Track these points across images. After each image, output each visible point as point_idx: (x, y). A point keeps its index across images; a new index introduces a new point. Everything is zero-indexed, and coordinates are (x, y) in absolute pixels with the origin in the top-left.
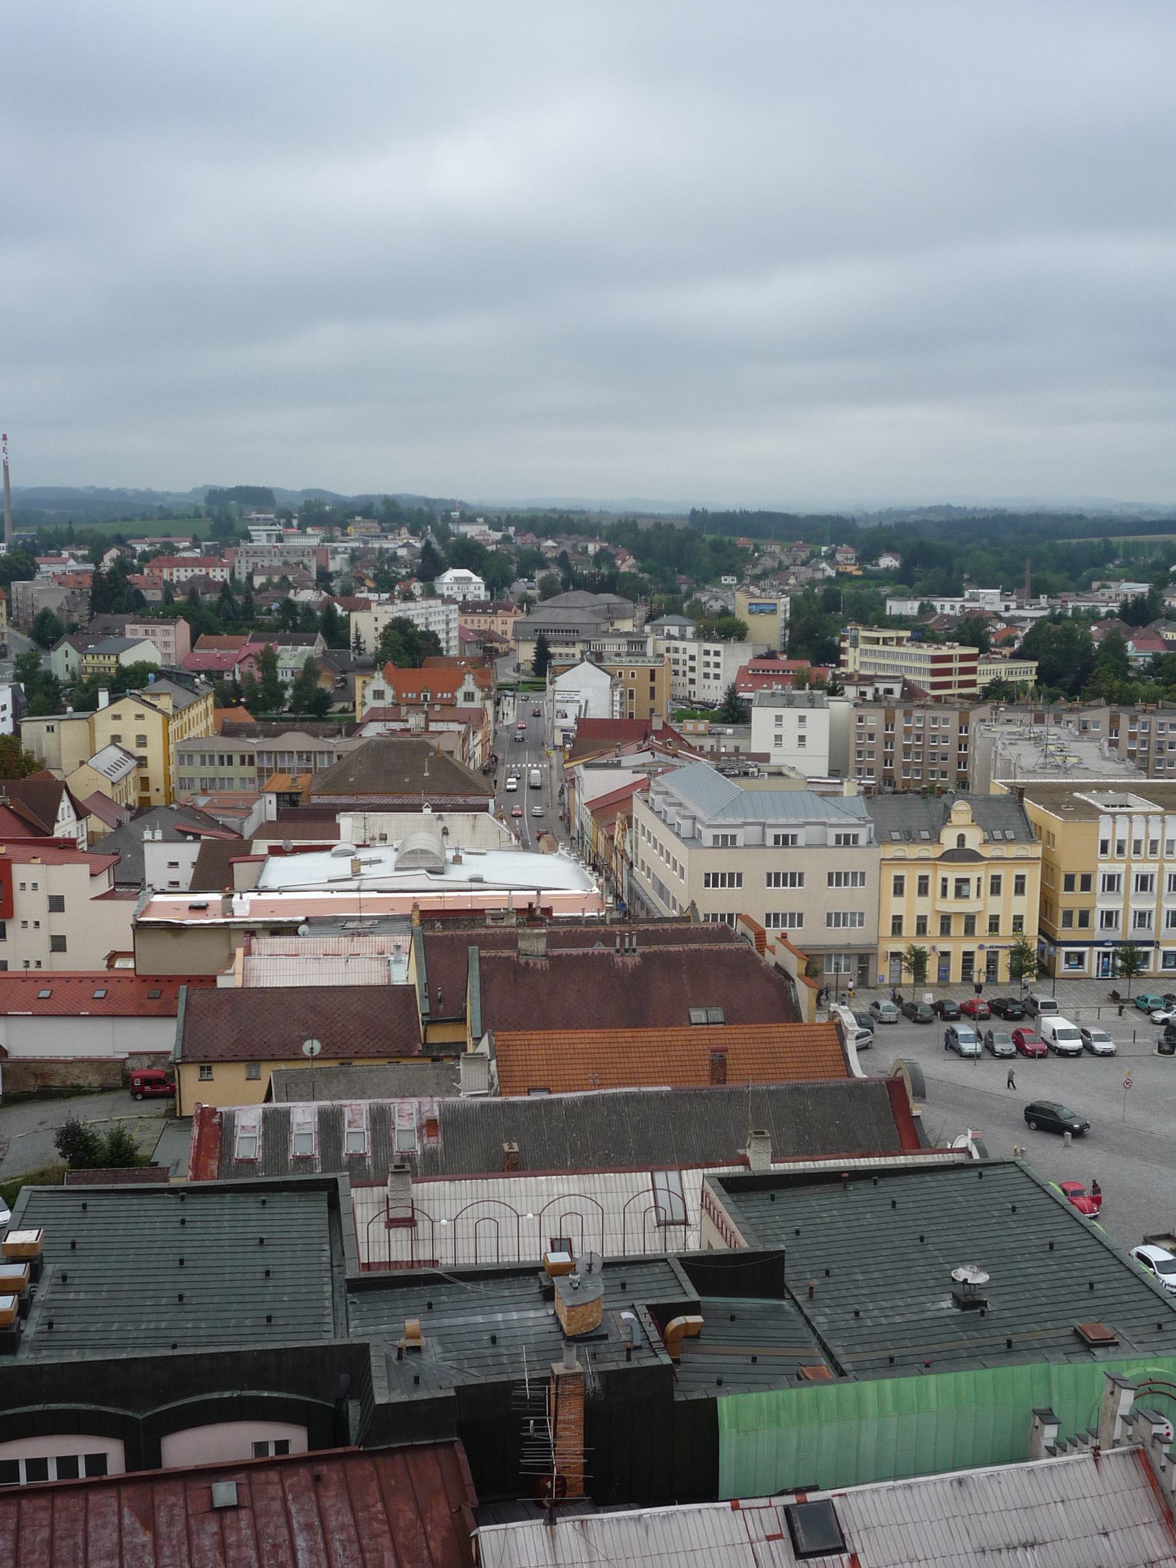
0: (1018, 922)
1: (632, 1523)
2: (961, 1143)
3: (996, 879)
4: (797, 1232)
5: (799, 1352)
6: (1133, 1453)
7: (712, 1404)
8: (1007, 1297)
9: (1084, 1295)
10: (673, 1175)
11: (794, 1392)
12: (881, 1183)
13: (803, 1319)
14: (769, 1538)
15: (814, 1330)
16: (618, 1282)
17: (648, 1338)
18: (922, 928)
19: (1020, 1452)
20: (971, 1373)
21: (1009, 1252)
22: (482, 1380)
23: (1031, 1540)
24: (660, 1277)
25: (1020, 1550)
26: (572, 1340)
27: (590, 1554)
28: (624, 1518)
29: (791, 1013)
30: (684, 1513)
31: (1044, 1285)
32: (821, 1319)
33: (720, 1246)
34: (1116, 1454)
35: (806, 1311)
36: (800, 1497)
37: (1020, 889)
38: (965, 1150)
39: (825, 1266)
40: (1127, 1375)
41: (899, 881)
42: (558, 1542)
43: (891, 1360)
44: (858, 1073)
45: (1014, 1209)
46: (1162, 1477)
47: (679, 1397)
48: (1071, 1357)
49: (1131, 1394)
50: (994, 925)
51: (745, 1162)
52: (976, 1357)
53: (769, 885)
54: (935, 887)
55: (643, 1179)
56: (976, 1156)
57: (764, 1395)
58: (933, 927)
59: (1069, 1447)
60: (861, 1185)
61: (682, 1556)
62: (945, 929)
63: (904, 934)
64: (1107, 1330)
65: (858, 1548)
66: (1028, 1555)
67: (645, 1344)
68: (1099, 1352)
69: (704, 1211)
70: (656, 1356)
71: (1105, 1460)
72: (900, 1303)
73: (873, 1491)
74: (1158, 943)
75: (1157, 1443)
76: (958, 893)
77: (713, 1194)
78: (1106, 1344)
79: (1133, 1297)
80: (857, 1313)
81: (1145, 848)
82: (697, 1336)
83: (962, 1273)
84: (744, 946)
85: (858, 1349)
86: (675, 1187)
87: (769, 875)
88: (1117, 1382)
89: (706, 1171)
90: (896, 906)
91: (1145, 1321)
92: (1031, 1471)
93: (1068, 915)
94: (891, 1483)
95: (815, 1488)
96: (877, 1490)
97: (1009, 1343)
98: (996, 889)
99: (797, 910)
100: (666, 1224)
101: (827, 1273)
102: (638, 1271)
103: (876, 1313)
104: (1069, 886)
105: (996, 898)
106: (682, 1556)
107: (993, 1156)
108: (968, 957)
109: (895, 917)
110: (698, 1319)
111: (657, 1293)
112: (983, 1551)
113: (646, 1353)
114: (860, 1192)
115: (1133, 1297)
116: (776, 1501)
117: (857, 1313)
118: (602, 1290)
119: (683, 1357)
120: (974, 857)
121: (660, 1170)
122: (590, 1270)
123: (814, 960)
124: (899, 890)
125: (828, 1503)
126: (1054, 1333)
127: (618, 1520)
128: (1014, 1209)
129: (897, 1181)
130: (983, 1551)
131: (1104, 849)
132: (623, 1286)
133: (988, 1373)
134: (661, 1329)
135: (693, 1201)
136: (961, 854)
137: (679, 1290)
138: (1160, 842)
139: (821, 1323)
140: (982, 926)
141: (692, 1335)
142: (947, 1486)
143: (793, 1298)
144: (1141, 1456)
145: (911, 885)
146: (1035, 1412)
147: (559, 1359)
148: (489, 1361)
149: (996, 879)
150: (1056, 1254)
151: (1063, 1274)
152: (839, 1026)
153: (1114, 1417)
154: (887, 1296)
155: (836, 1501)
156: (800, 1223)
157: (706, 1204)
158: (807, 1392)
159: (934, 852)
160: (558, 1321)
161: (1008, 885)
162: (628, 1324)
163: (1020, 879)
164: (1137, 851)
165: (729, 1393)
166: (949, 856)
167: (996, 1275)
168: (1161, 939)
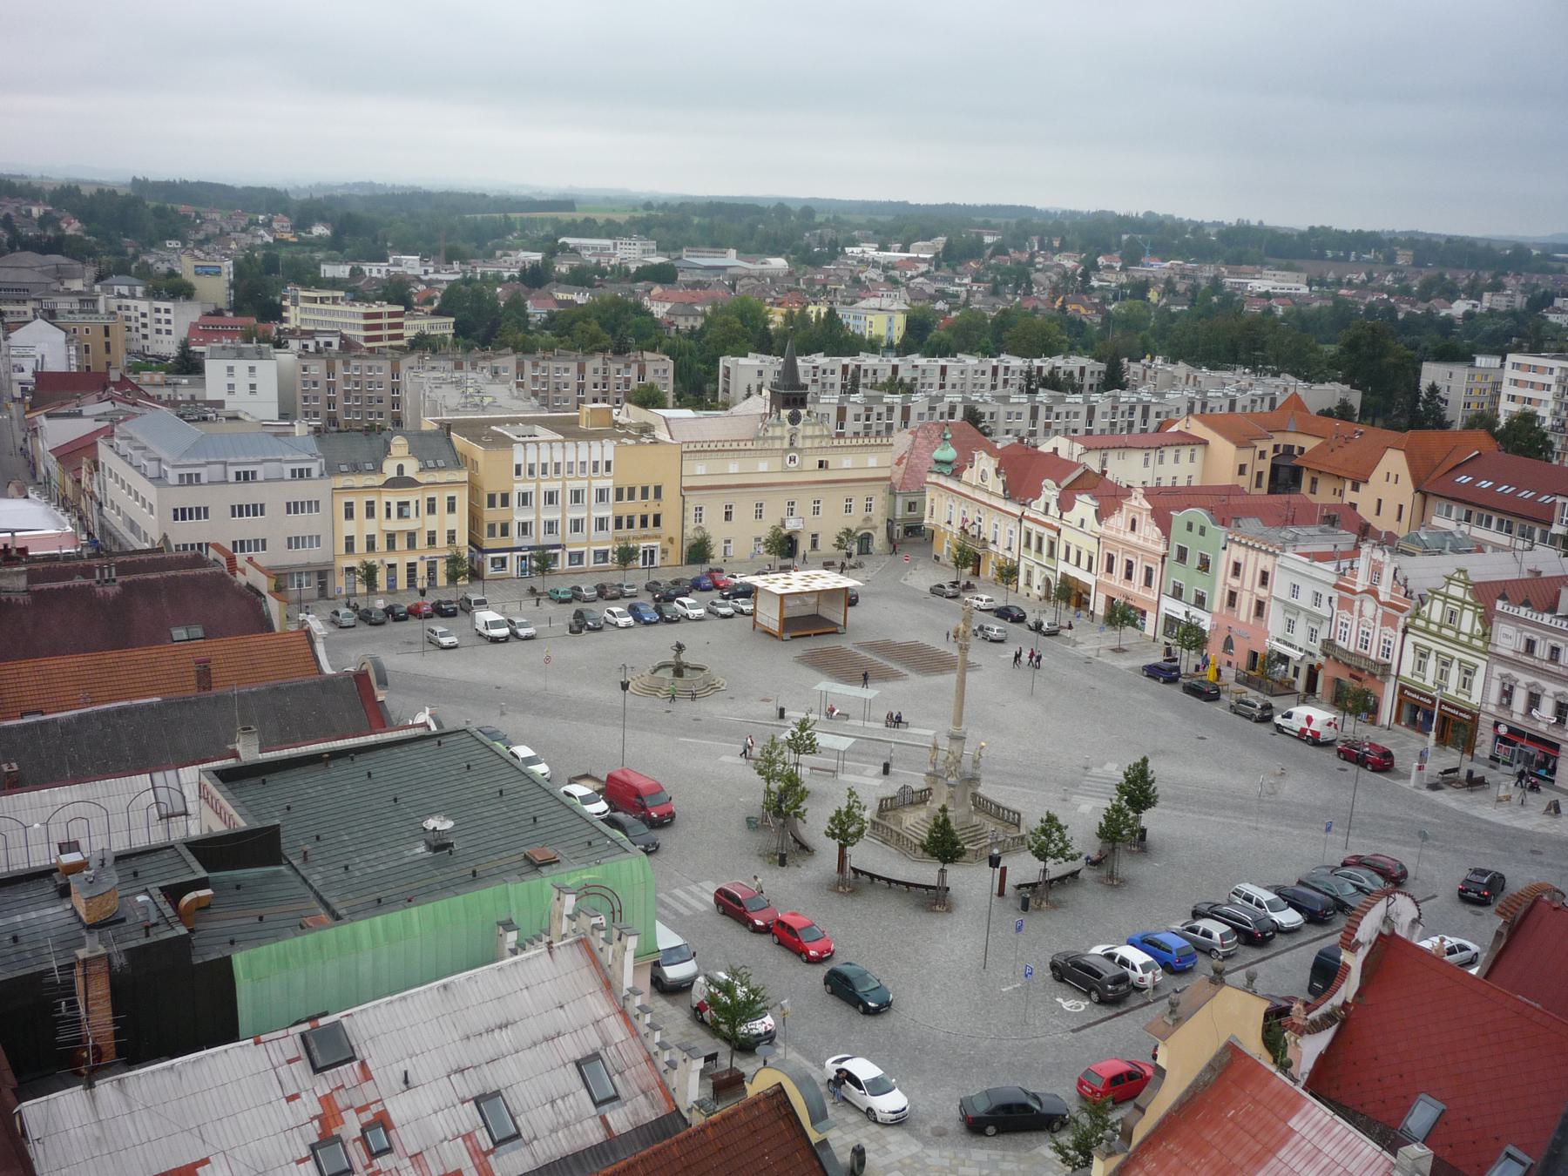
0: (451, 536)
1: (166, 1073)
2: (421, 718)
3: (431, 501)
4: (289, 808)
5: (301, 906)
6: (577, 942)
7: (227, 963)
8: (470, 838)
9: (530, 828)
10: (170, 774)
11: (299, 940)
12: (357, 758)
13: (300, 879)
14: (289, 1062)
15: (311, 887)
16: (130, 871)
17: (163, 915)
18: (371, 545)
19: (489, 956)
20: (445, 902)
21: (468, 802)
22: (9, 976)
23: (505, 1022)
24: (170, 861)
25: (497, 1031)
26: (90, 927)
27: (129, 1105)
28: (158, 1070)
29: (265, 625)
30: (213, 1056)
31: (497, 824)
32: (317, 877)
33: (219, 828)
34: (565, 945)
35: (303, 873)
36: (313, 1023)
37: (451, 508)
38: (425, 725)
39: (315, 833)
40: (568, 884)
41: (349, 505)
42: (98, 1102)
43: (379, 901)
44: (328, 670)
45: (469, 767)
46: (601, 956)
47: (197, 960)
48: (524, 877)
49: (573, 897)
50: (432, 540)
51: (235, 755)
52: (449, 888)
53: (234, 516)
54: (380, 510)
55: (143, 780)
56: (434, 728)
57: (273, 946)
58: (381, 543)
59: (528, 946)
60: (339, 762)
61: (214, 1091)
62: (391, 545)
64: (550, 852)
65: (366, 1055)
66: (504, 1033)
67: (162, 920)
68: (545, 870)
69: (202, 801)
70: (173, 928)
71: (557, 951)
72: (382, 854)
73: (374, 1007)
75: (595, 931)
76: (400, 514)
77: (209, 785)
78: (549, 863)
79: (567, 824)
80: (346, 868)
82: (208, 907)
83: (432, 823)
84: (217, 569)
85: (350, 896)
86: (172, 782)
88: (562, 890)
89: (200, 766)
90: (348, 528)
91: (579, 841)
92: (500, 969)
93: (492, 527)
94: (388, 999)
95: (325, 1014)
96: (378, 1006)
97: (474, 873)
98: (431, 509)
100: (168, 817)
101: (318, 838)
102: (148, 860)
103: (362, 865)
104: (492, 503)
105: (432, 517)
106: (214, 1091)
107: (448, 727)
108: (412, 568)
109: (347, 538)
110: (208, 892)
111: (167, 875)
112: (468, 1038)
113: (162, 928)
114: (338, 769)
115: (567, 824)
116: (292, 1030)
117: (346, 868)
118: (116, 881)
119: (198, 926)
120: (411, 483)
121: (158, 770)
122: (103, 865)
123: (281, 579)
124: (349, 514)
125: (337, 1024)
126: (507, 861)
127: (153, 1072)
128: (469, 767)
129: (370, 755)
130: (468, 1038)
131: (518, 472)
132: (135, 874)
133: (460, 898)
134: (175, 904)
135: (191, 793)
136: (401, 481)
137: (187, 870)
139: (316, 879)
140: (421, 541)
141: (203, 907)
142: (435, 992)
143: (290, 863)
144: (583, 943)
145: (360, 510)
146: (499, 924)
147: (82, 945)
148: (13, 958)
149: (431, 501)
150: (505, 798)
151: (512, 814)
152: (308, 632)
153: (561, 917)
154: (371, 850)
155: (344, 1021)
156: (289, 800)
157: (203, 794)
158: (310, 938)
159: (378, 480)
160: (76, 914)
161: (441, 505)
162: (143, 906)
163: (451, 500)
164: (544, 473)
165: (241, 949)
166: (391, 484)
167: (458, 821)
168: (567, 542)
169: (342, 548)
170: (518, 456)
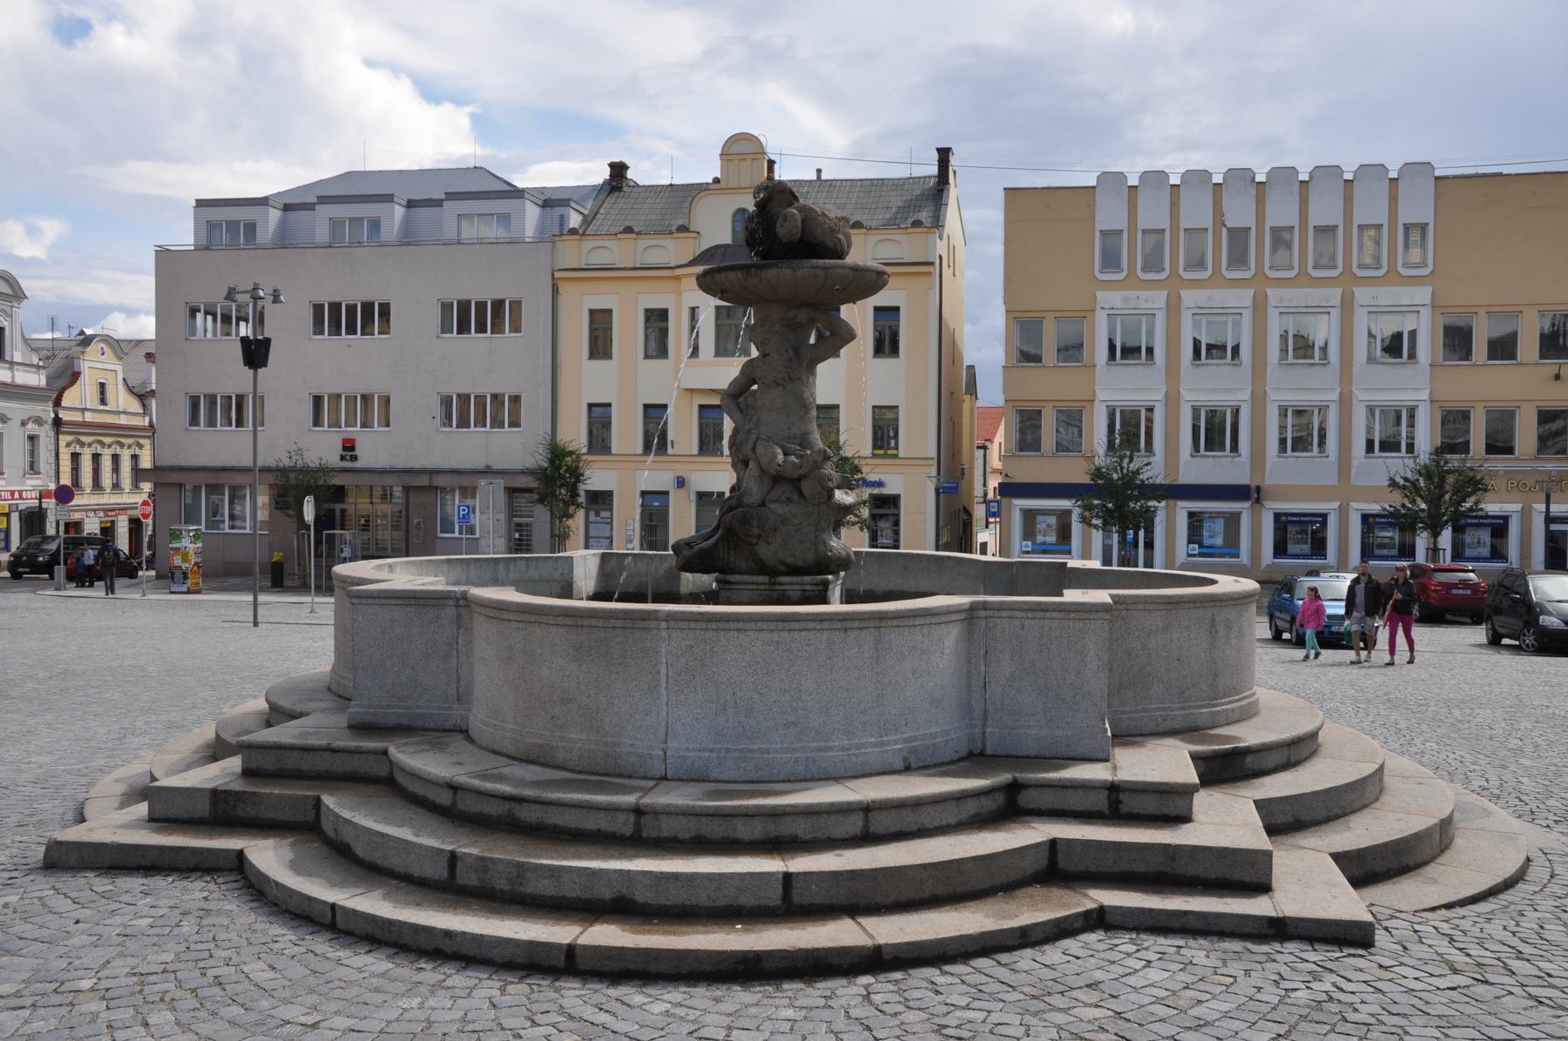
18: (656, 440)
41: (600, 323)
63: (614, 450)
74: (1258, 489)
81: (1216, 249)
87: (318, 309)
99: (376, 388)
124: (600, 346)
138: (1253, 233)
145: (628, 333)
168: (1270, 480)
169: (575, 434)
170: (1110, 215)
